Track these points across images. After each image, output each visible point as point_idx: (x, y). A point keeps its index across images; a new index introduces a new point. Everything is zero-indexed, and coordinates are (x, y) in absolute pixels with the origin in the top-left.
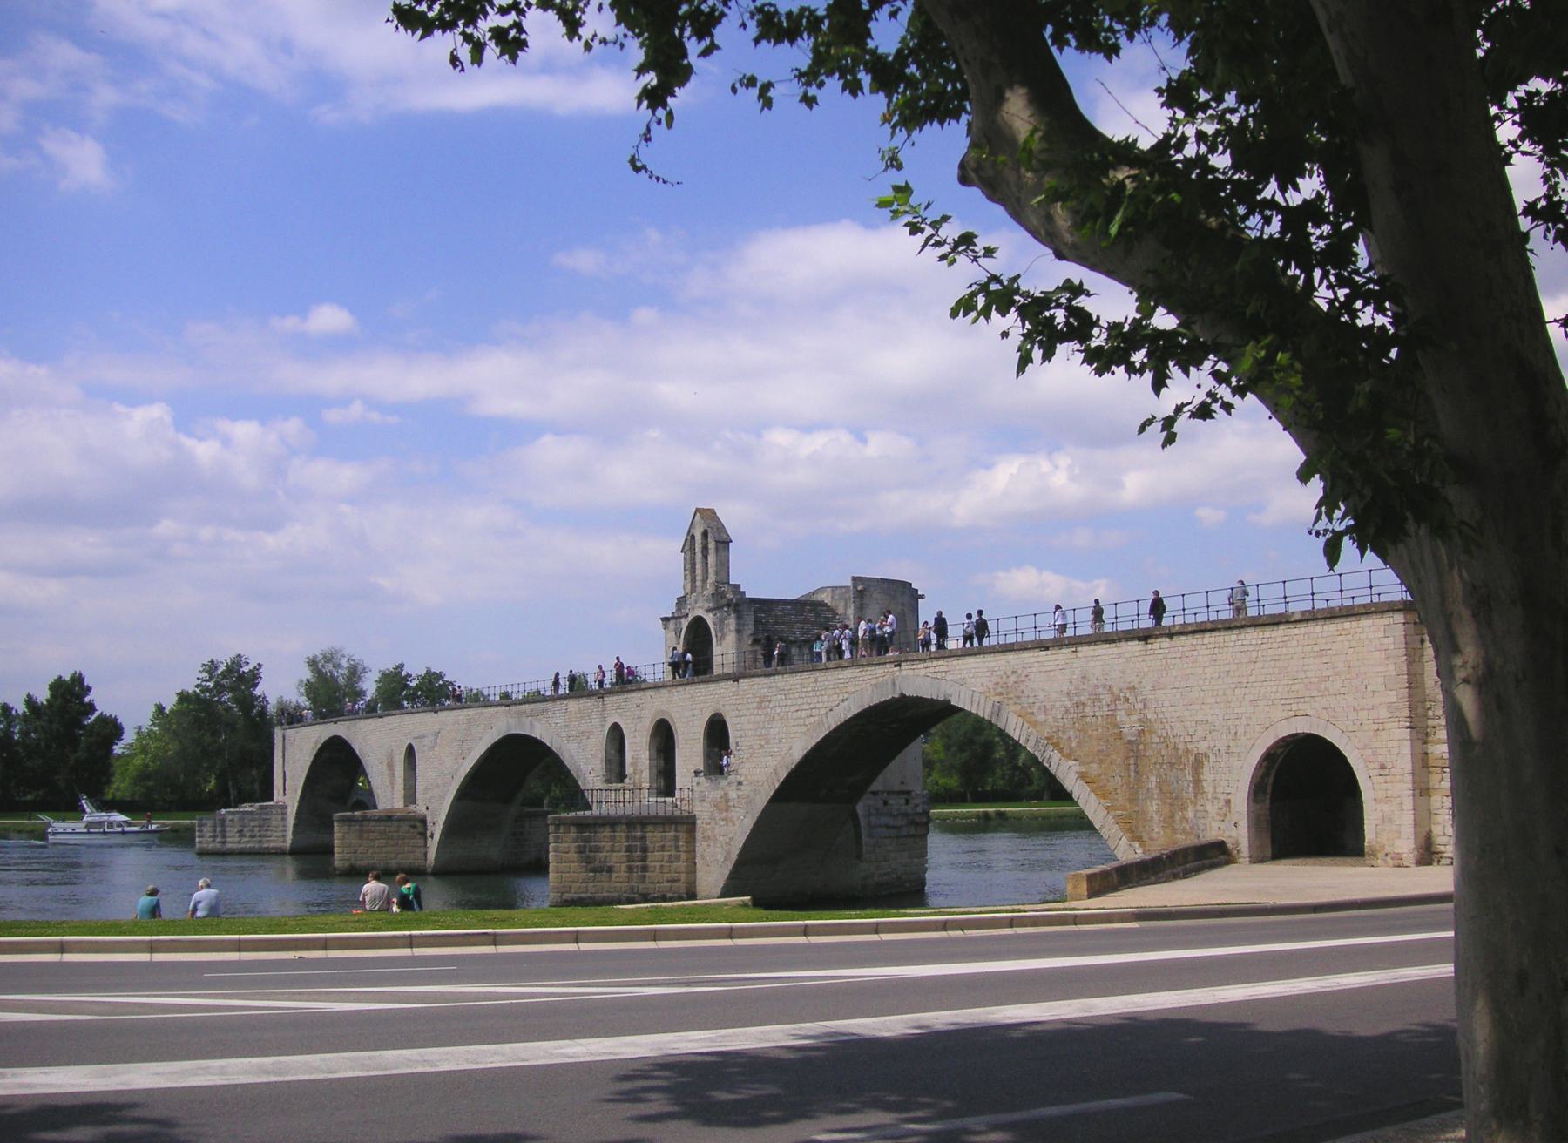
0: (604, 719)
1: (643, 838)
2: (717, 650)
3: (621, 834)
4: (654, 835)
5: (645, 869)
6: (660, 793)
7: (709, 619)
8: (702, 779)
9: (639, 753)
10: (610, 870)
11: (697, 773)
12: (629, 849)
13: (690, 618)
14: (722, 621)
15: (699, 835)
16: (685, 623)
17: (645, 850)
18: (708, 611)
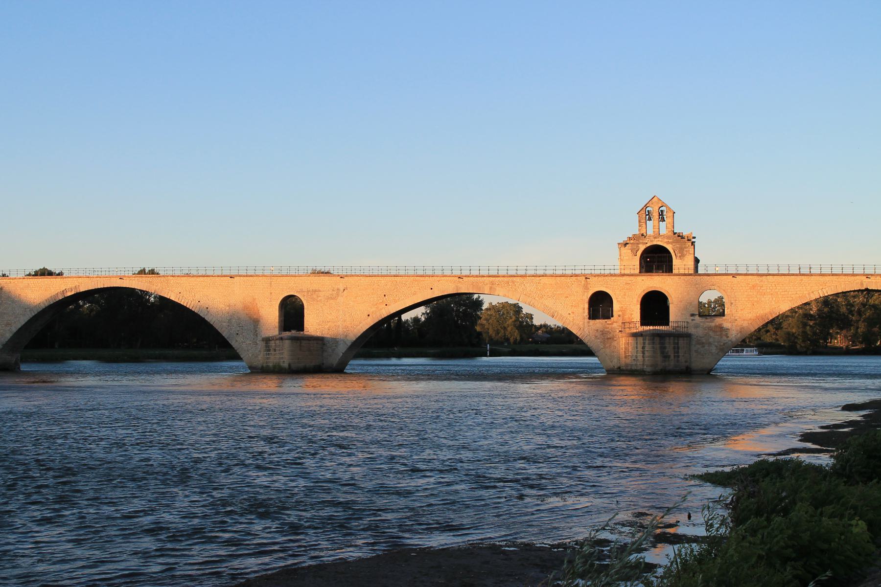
0: (586, 288)
1: (678, 343)
2: (676, 262)
3: (672, 341)
4: (681, 342)
5: (678, 357)
6: (642, 324)
7: (669, 247)
8: (697, 317)
9: (627, 307)
10: (669, 357)
11: (692, 315)
12: (674, 348)
13: (648, 245)
14: (681, 250)
15: (694, 343)
16: (642, 248)
17: (678, 348)
18: (668, 243)
